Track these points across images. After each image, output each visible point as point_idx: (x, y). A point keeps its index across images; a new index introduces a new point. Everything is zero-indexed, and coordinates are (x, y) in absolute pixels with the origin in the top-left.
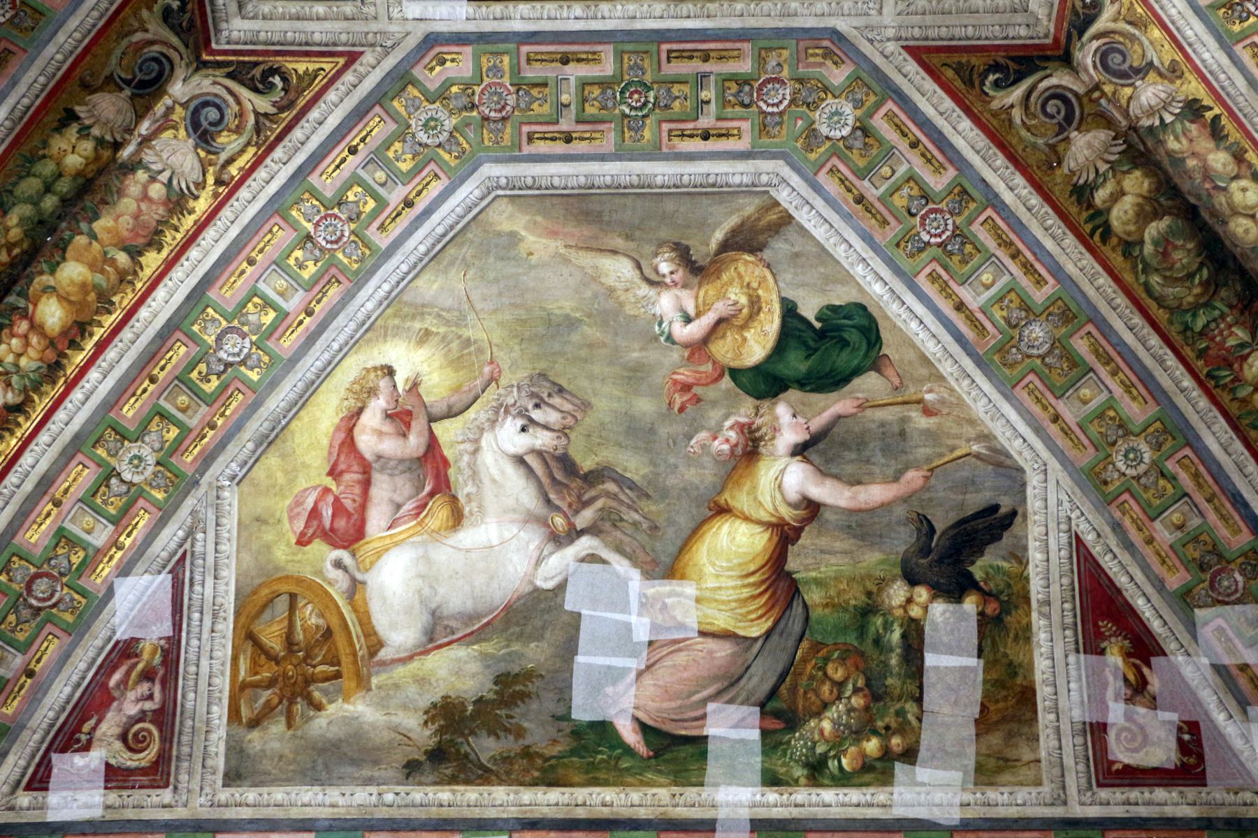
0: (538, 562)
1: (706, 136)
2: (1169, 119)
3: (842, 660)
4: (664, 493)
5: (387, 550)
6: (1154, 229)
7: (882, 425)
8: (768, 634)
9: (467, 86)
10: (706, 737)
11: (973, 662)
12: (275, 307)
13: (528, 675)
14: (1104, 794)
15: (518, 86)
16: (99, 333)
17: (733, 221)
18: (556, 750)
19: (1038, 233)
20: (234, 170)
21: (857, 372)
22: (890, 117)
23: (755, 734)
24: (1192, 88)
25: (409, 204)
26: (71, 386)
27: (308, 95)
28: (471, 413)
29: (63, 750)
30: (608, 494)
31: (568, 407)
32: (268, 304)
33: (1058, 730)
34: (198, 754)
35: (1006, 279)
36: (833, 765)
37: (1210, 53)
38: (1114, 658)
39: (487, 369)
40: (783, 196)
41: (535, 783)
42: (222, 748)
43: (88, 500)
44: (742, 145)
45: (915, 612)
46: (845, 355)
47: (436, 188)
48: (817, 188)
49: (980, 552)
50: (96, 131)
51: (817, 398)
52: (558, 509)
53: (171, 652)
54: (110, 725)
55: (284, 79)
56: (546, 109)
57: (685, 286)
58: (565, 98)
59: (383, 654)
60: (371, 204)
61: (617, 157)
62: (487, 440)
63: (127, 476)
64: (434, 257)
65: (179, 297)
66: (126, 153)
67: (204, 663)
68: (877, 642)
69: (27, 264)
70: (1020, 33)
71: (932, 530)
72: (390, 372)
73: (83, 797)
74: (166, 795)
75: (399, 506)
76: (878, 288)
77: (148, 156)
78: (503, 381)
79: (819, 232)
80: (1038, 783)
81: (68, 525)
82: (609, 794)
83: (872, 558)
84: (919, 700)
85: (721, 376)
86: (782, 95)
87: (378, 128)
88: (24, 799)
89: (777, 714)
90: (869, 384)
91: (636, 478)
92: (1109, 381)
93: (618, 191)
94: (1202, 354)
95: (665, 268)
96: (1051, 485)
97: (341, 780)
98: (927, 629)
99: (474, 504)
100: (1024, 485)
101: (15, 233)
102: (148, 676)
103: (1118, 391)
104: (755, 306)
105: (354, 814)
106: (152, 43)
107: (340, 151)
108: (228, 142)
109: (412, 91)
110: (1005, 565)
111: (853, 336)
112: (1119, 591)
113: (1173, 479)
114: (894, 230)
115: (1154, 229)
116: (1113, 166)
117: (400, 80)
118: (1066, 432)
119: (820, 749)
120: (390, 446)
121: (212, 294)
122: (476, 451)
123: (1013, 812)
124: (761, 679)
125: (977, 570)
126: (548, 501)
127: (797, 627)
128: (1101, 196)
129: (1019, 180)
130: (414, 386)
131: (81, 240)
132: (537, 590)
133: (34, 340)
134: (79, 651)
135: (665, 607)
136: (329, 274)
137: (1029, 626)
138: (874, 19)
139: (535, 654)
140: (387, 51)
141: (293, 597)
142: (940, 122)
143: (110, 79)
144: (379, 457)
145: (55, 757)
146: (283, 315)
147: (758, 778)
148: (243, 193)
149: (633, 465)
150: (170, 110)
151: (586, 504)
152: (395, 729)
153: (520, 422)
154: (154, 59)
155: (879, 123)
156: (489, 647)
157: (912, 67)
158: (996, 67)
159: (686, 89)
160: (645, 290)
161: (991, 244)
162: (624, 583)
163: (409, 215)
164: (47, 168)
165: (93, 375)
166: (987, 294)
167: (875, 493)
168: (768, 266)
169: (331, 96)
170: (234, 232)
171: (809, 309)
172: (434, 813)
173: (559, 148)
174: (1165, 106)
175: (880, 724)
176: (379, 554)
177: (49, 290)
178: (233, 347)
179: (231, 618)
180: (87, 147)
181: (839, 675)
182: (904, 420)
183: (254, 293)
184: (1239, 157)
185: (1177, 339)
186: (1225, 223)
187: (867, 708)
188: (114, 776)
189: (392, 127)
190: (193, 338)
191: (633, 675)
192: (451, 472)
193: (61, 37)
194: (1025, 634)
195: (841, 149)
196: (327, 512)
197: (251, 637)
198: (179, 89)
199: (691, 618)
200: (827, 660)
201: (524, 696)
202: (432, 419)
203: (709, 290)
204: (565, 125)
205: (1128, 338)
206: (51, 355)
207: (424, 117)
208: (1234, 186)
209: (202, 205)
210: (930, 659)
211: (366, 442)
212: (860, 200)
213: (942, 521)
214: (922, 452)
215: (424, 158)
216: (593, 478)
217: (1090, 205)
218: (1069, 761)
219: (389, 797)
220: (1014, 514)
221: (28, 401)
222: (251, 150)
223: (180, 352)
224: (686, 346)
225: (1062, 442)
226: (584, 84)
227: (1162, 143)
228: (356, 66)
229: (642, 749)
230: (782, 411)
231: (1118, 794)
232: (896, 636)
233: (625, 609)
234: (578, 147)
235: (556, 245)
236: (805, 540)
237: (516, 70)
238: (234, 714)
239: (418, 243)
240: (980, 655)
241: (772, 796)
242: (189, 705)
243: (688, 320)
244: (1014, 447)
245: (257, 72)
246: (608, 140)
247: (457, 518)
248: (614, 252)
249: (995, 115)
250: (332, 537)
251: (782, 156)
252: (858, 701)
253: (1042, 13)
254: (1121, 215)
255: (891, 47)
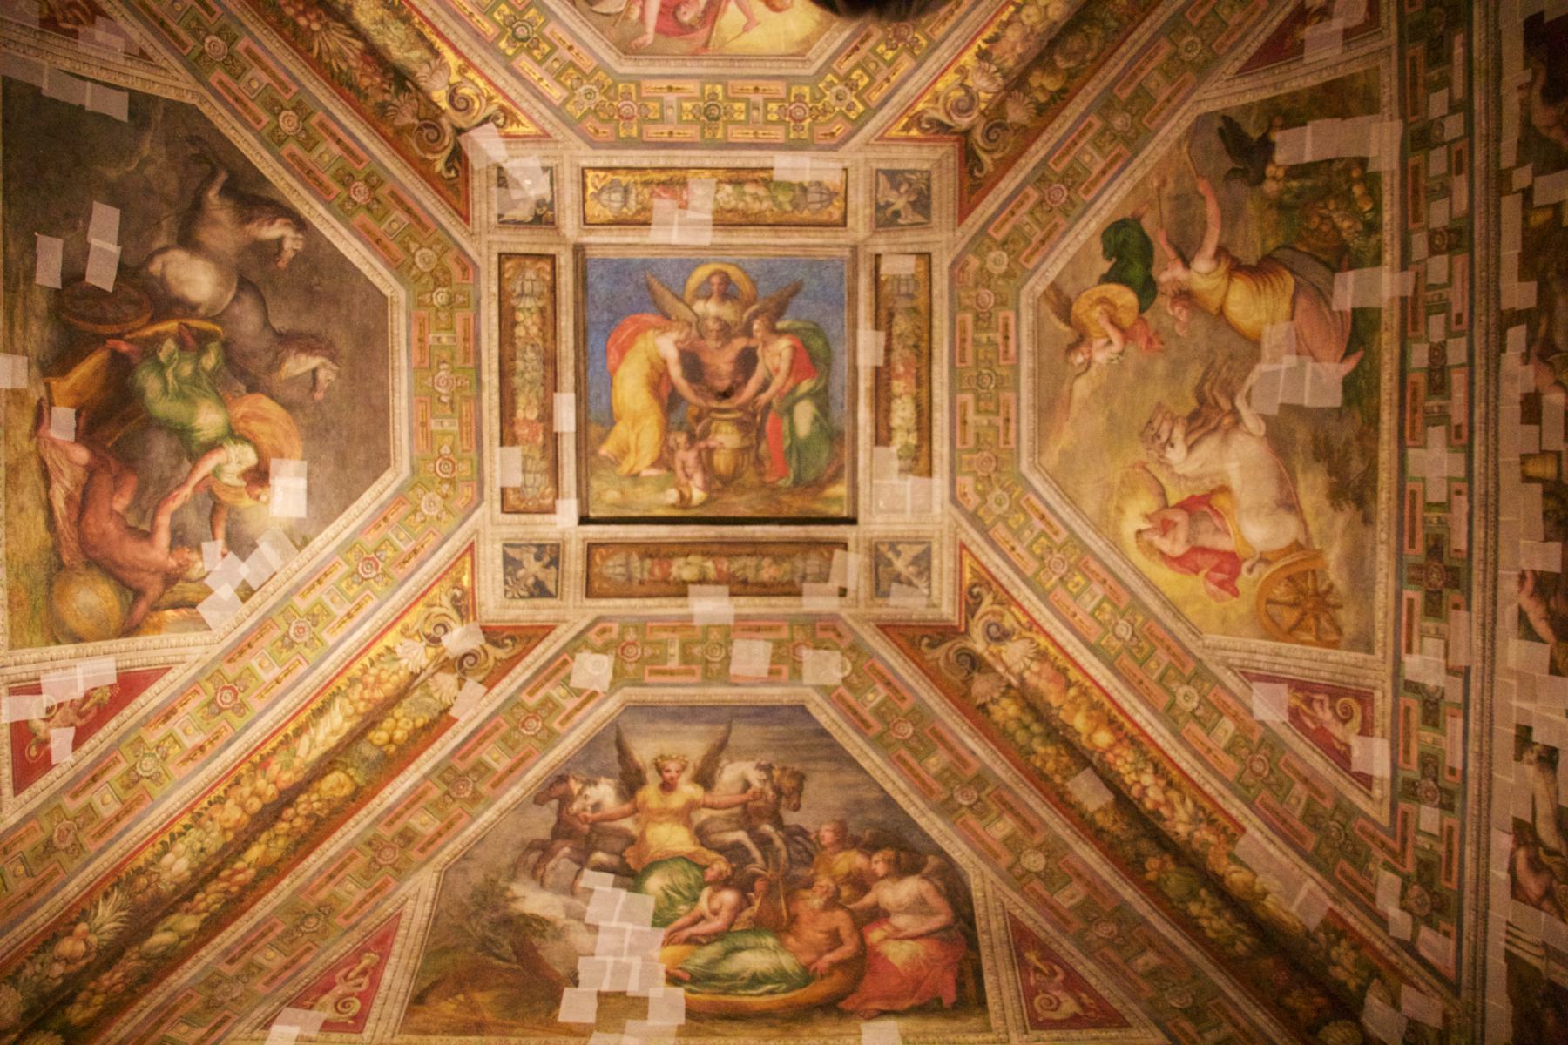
0: (1250, 434)
1: (1006, 338)
2: (994, 68)
3: (1308, 218)
4: (1211, 351)
5: (1242, 537)
6: (1061, 63)
7: (1171, 212)
8: (1293, 272)
9: (978, 480)
10: (1354, 310)
11: (1309, 129)
12: (1101, 602)
13: (1315, 438)
14: (1384, 20)
15: (979, 450)
16: (1114, 712)
17: (1053, 317)
18: (1358, 417)
19: (1062, 131)
20: (1024, 620)
21: (1142, 232)
22: (997, 229)
23: (1351, 275)
24: (968, 59)
25: (1043, 517)
26: (1144, 733)
27: (983, 573)
28: (1163, 481)
29: (1349, 762)
30: (1211, 389)
31: (1159, 418)
32: (1099, 607)
33: (1349, 61)
34: (1354, 671)
35: (1088, 148)
36: (1369, 217)
37: (944, 53)
38: (1308, 32)
39: (1138, 470)
40: (1040, 289)
41: (1377, 430)
42: (1352, 654)
43: (1209, 731)
44: (1012, 315)
45: (1280, 173)
46: (1131, 241)
47: (1034, 500)
48: (1037, 268)
49: (1245, 136)
50: (996, 695)
51: (1157, 254)
52: (1220, 422)
53: (1299, 686)
54: (1337, 730)
55: (975, 585)
56: (991, 432)
57: (1090, 345)
58: (985, 422)
59: (1302, 540)
60: (1043, 539)
61: (1017, 390)
62: (1179, 470)
63: (1195, 704)
64: (1073, 502)
65: (1095, 661)
66: (1015, 682)
67: (1305, 664)
68: (1298, 196)
69: (1075, 748)
70: (952, 162)
71: (1234, 170)
72: (1139, 532)
73: (1377, 753)
74: (1378, 694)
75: (1217, 530)
76: (1093, 225)
77: (1016, 669)
78: (1145, 459)
79: (1061, 264)
80: (1378, 68)
81: (1223, 745)
82: (1385, 377)
83: (1250, 208)
84: (1330, 162)
85: (1145, 321)
86: (987, 297)
87: (1000, 533)
88: (1377, 792)
89: (1339, 260)
90: (1148, 224)
91: (1202, 370)
92: (1145, 73)
93: (1037, 389)
94: (1131, 18)
95: (1080, 359)
96: (1206, 96)
97: (1372, 570)
98: (1292, 163)
99: (1217, 478)
100: (1207, 114)
101: (1051, 750)
102: (1309, 702)
103: (1152, 65)
104: (1103, 300)
105: (1393, 562)
106: (947, 657)
107: (1011, 555)
108: (1008, 622)
109: (981, 513)
110: (1253, 118)
111: (1121, 237)
112: (1269, 39)
113: (1204, 19)
114: (1059, 219)
115: (1061, 63)
116: (1026, 94)
117: (974, 519)
118: (1175, 93)
119: (1360, 227)
120: (1181, 533)
121: (1093, 640)
122: (1185, 477)
123: (1395, 83)
124: (1318, 274)
125: (1255, 135)
126: (1215, 429)
127: (1288, 253)
128: (1042, 98)
129: (1033, 148)
130: (1148, 517)
131: (1062, 715)
132: (1266, 435)
133: (1117, 751)
134: (1294, 747)
135: (1278, 346)
136: (1080, 567)
137: (1289, 95)
138: (944, 244)
139: (1302, 434)
140: (959, 525)
141: (1269, 602)
142: (1000, 200)
143: (964, 682)
144: (1188, 541)
145: (1354, 769)
146: (1105, 598)
147: (1376, 270)
148: (1036, 616)
149: (1194, 373)
150: (992, 654)
151: (1217, 403)
152: (1344, 532)
153: (1169, 449)
154: (958, 656)
155: (999, 236)
156: (1299, 468)
157: (969, 220)
158: (971, 172)
159: (981, 351)
160: (1093, 371)
161: (1068, 158)
162: (1264, 375)
163: (1049, 517)
164: (1012, 726)
165: (1137, 718)
166: (1097, 157)
167: (1212, 210)
168: (1079, 294)
169: (984, 559)
170: (1057, 623)
171: (1104, 266)
172: (1394, 503)
173: (1013, 425)
174: (985, 71)
175: (1345, 187)
176: (1246, 543)
177: (1090, 737)
178: (1124, 630)
179: (1278, 644)
180: (1005, 702)
181: (1316, 219)
182: (1170, 199)
183: (1092, 614)
184: (1008, 23)
185: (1123, 34)
186: (1055, 23)
187: (1337, 197)
188: (1366, 730)
189: (1000, 525)
190: (1118, 655)
191: (1317, 365)
192: (1197, 493)
193: (931, 702)
194: (1294, 96)
195: (1014, 256)
196: (1219, 576)
197: (1291, 631)
198: (979, 645)
199: (1284, 326)
200: (1307, 229)
201: (1327, 440)
202: (1166, 506)
203: (1093, 329)
204: (1000, 422)
205: (1121, 65)
206: (1126, 742)
207: (995, 506)
208: (1028, 22)
209: (1043, 642)
210: (1308, 158)
211: (1179, 549)
212: (1043, 242)
213: (1227, 163)
214: (1187, 183)
215: (1016, 507)
216: (1202, 400)
217: (1047, 104)
218: (1365, 50)
219: (1384, 536)
220: (1224, 117)
221: (1151, 760)
222: (1014, 609)
223: (1127, 661)
224: (1125, 342)
225: (1181, 95)
226: (978, 411)
227: (1011, 69)
228: (968, 543)
229: (1360, 354)
230: (1163, 277)
231: (1384, 10)
232: (1294, 184)
233: (1277, 373)
234: (1013, 416)
235: (1067, 425)
236: (1239, 254)
237: (970, 451)
238: (1333, 645)
239: (1065, 512)
240: (1304, 124)
241: (1387, 257)
242: (1327, 675)
243: (1110, 342)
244: (1185, 124)
245: (971, 601)
246: (1009, 395)
247: (1225, 489)
248: (1071, 391)
249: (996, 168)
250: (1235, 574)
251: (1019, 289)
252: (1332, 205)
253: (941, 151)
254: (1052, 84)
255: (959, 234)
